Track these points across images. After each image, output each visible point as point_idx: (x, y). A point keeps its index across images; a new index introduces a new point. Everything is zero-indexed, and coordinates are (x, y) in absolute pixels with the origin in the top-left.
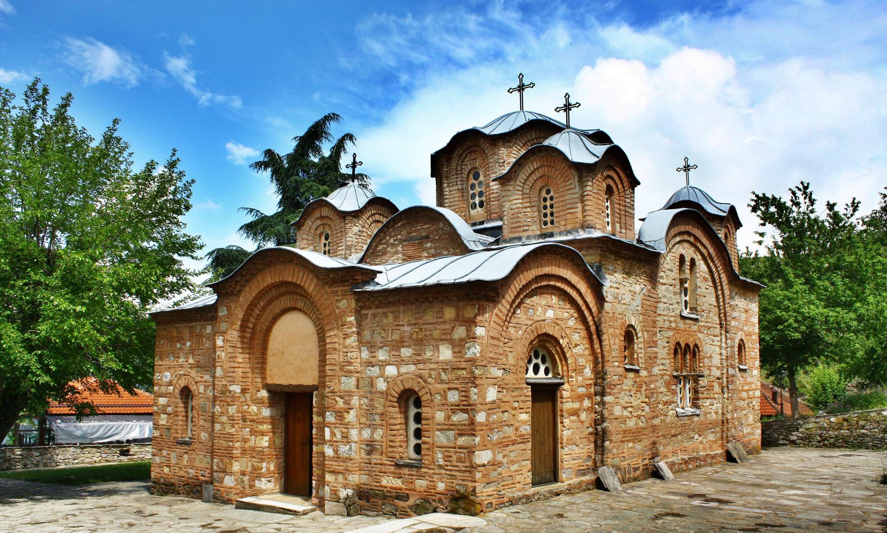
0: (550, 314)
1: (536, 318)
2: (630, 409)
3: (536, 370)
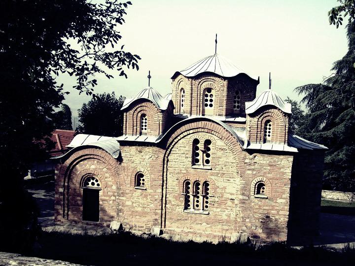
0: (93, 167)
1: (85, 168)
2: (138, 204)
3: (93, 184)
